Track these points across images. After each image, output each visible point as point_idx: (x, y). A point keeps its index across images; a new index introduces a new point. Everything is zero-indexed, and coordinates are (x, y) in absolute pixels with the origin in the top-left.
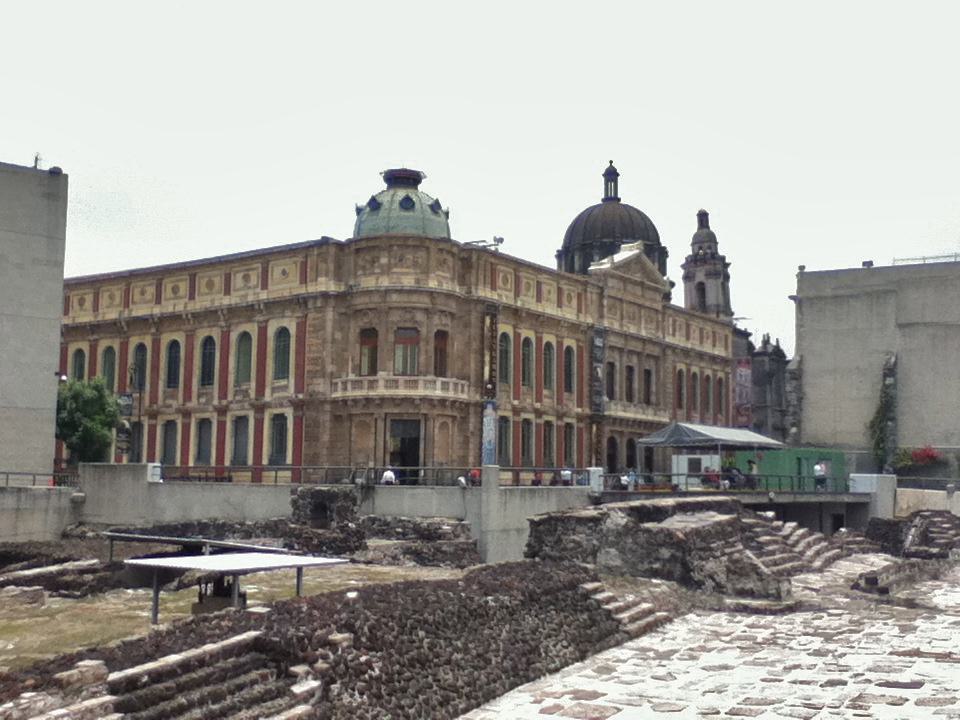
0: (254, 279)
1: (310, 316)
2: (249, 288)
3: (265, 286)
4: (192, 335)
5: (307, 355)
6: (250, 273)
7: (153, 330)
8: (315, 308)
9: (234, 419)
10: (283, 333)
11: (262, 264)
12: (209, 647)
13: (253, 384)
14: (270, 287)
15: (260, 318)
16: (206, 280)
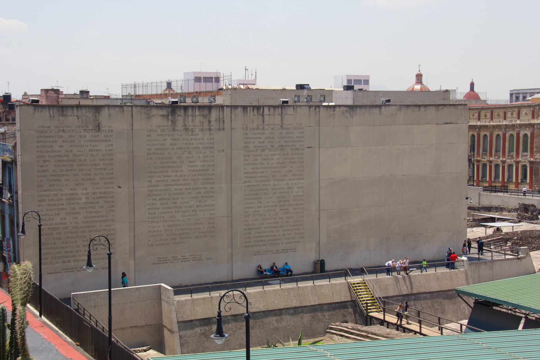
0: (515, 115)
1: (535, 131)
2: (513, 118)
3: (519, 118)
4: (492, 134)
5: (534, 145)
6: (513, 112)
7: (478, 130)
8: (537, 128)
9: (508, 165)
10: (526, 135)
11: (517, 109)
12: (495, 238)
13: (515, 153)
14: (521, 118)
15: (517, 130)
16: (497, 113)
